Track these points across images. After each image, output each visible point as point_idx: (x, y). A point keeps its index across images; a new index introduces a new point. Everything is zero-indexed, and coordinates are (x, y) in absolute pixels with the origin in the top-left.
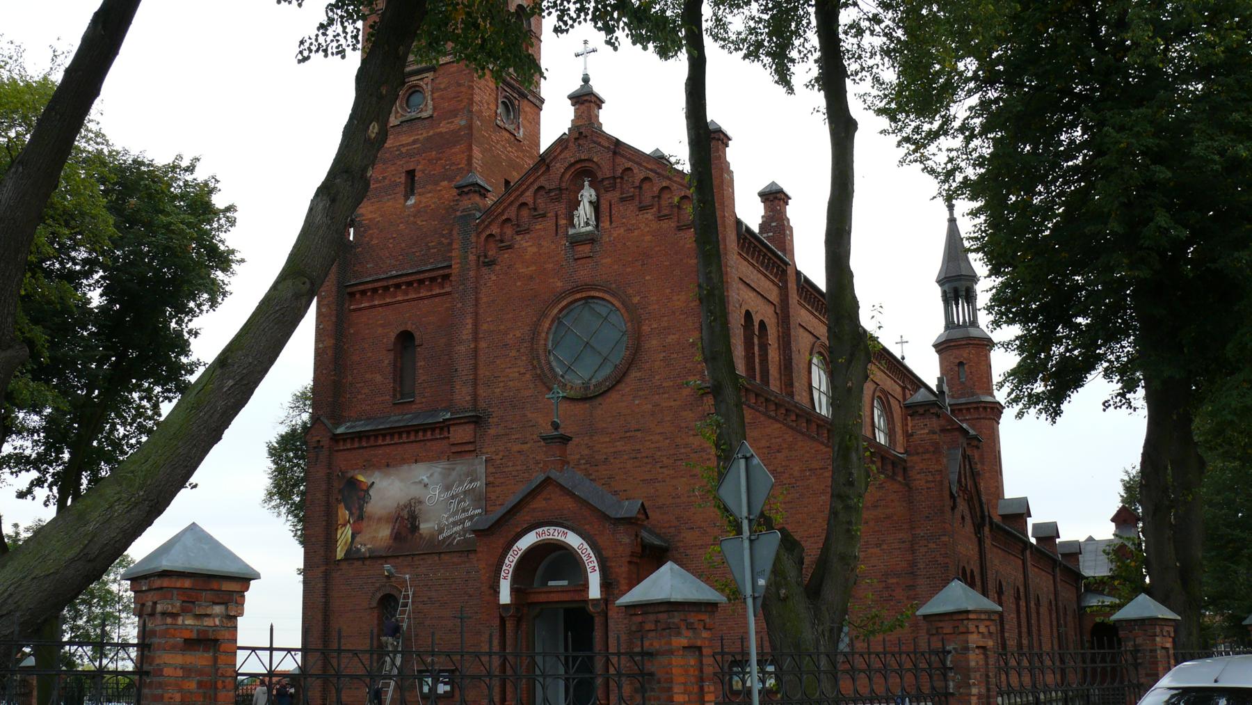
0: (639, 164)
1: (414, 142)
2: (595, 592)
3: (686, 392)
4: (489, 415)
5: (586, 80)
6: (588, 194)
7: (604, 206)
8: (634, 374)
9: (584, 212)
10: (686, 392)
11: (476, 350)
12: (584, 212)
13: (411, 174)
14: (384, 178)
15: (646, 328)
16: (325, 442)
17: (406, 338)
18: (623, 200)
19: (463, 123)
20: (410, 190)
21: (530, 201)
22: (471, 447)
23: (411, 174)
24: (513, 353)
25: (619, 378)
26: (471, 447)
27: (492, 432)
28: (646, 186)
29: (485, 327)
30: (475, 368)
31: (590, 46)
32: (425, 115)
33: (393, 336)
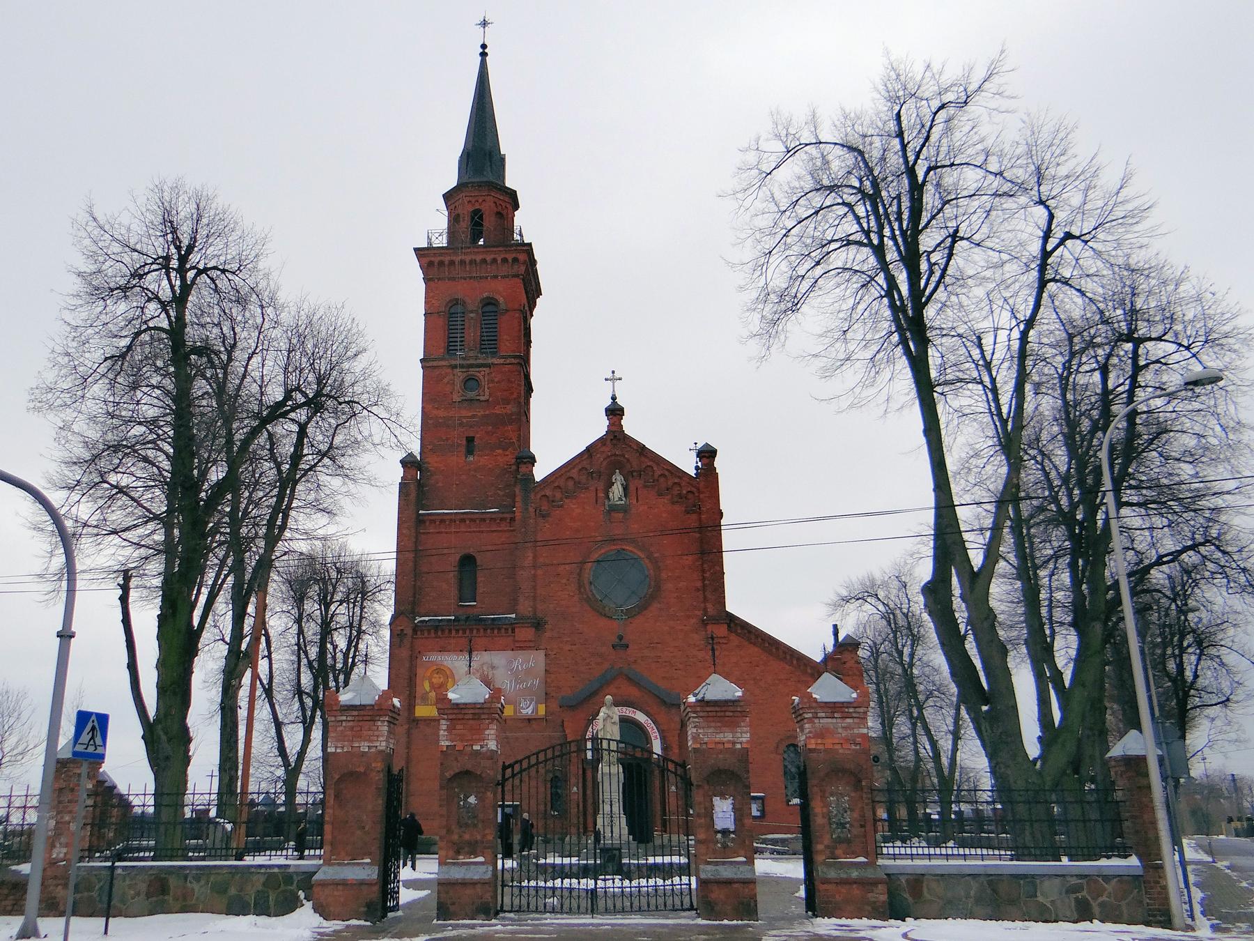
0: (658, 464)
1: (473, 416)
2: (657, 747)
3: (693, 621)
4: (546, 623)
5: (614, 398)
6: (618, 479)
7: (632, 488)
8: (656, 605)
9: (617, 491)
10: (693, 621)
11: (535, 576)
12: (617, 491)
13: (470, 440)
14: (447, 439)
15: (664, 575)
16: (409, 631)
17: (468, 562)
18: (645, 487)
19: (514, 410)
20: (470, 452)
21: (575, 476)
22: (532, 644)
23: (470, 440)
24: (564, 581)
25: (643, 607)
26: (532, 644)
27: (548, 634)
28: (662, 480)
29: (541, 560)
30: (534, 588)
31: (617, 375)
32: (482, 398)
33: (458, 557)
